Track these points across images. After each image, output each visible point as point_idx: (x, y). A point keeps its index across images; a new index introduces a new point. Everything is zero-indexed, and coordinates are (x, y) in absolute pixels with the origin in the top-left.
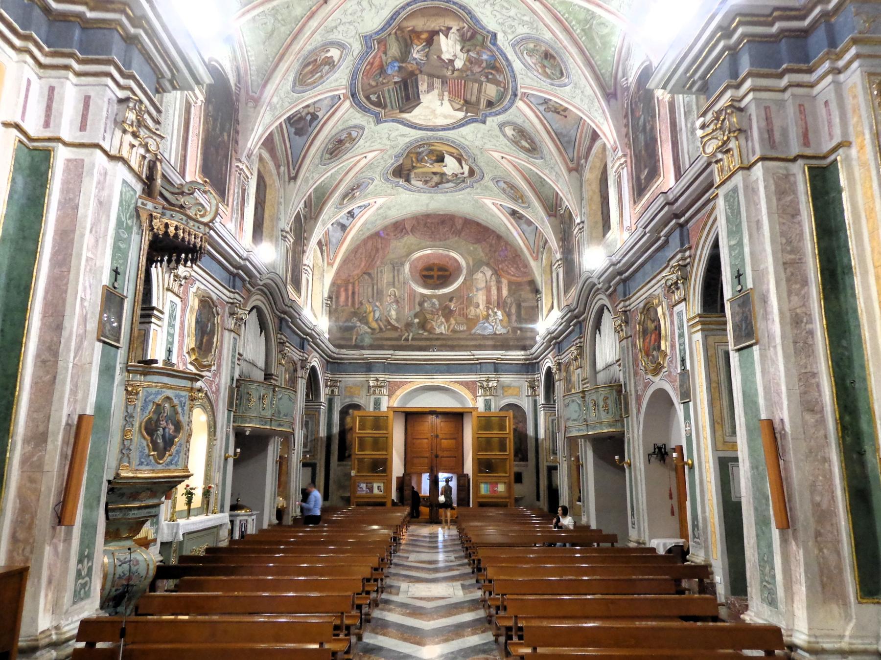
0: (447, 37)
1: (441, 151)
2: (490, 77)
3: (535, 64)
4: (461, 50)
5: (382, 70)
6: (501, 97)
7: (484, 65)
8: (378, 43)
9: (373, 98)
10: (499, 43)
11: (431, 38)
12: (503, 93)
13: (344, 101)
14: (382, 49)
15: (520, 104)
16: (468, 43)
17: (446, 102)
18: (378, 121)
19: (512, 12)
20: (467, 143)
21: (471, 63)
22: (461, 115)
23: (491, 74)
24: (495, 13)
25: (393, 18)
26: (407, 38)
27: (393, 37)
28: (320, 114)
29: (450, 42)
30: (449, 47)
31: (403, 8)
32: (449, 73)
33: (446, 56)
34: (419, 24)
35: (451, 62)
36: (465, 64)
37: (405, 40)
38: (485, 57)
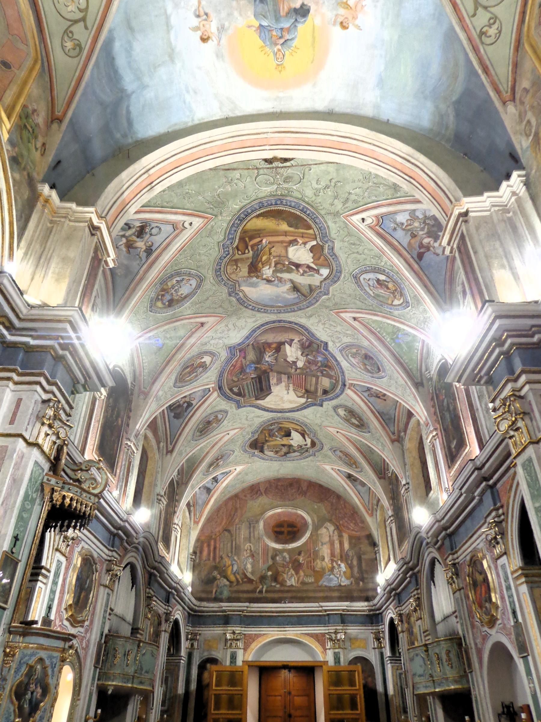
0: (291, 346)
1: (288, 428)
2: (324, 372)
4: (302, 355)
5: (242, 370)
6: (334, 387)
8: (240, 351)
9: (235, 390)
10: (329, 349)
11: (279, 347)
12: (335, 384)
13: (213, 392)
14: (243, 355)
15: (349, 392)
16: (307, 350)
18: (239, 407)
19: (339, 328)
20: (308, 421)
21: (309, 363)
22: (303, 400)
27: (251, 347)
28: (194, 403)
29: (293, 349)
30: (292, 352)
31: (259, 328)
32: (293, 371)
33: (290, 359)
34: (271, 338)
35: (295, 363)
36: (304, 364)
38: (320, 359)
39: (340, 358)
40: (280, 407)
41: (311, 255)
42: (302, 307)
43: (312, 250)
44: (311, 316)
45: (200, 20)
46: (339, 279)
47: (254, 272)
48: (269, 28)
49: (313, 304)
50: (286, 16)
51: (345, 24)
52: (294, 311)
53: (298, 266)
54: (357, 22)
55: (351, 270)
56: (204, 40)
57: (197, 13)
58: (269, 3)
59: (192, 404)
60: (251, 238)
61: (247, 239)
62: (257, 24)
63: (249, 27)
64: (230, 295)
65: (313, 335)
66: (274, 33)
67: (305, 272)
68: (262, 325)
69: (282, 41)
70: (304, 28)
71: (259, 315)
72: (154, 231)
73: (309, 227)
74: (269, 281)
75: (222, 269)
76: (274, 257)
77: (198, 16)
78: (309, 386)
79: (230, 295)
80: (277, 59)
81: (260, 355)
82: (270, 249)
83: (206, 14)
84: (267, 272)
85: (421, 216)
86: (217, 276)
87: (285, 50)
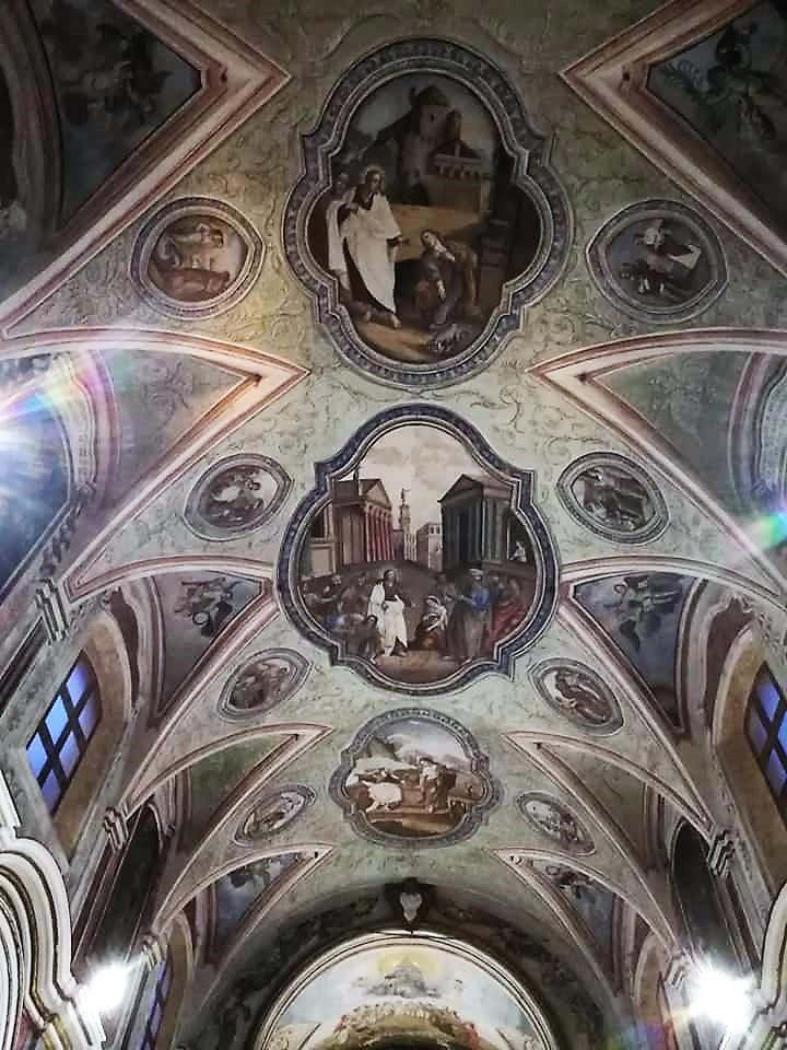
0: (397, 640)
1: (407, 323)
3: (270, 666)
4: (376, 619)
5: (496, 599)
6: (303, 564)
7: (340, 607)
9: (521, 553)
10: (325, 654)
11: (420, 636)
13: (572, 582)
14: (488, 641)
15: (270, 573)
16: (368, 635)
17: (396, 503)
18: (527, 478)
19: (318, 705)
20: (346, 376)
23: (326, 596)
24: (337, 692)
25: (466, 679)
26: (449, 641)
27: (472, 654)
30: (393, 623)
31: (451, 688)
33: (399, 605)
34: (434, 662)
35: (389, 597)
37: (455, 641)
38: (341, 620)
39: (305, 648)
40: (425, 431)
41: (371, 796)
42: (379, 720)
43: (372, 801)
44: (367, 706)
46: (332, 780)
47: (450, 776)
49: (362, 730)
52: (392, 712)
53: (388, 779)
55: (318, 802)
59: (625, 580)
60: (447, 815)
61: (451, 815)
64: (487, 758)
65: (358, 671)
67: (379, 774)
68: (445, 690)
71: (448, 711)
72: (555, 871)
73: (373, 824)
74: (429, 760)
75: (488, 800)
76: (419, 790)
78: (356, 527)
79: (487, 758)
81: (455, 629)
82: (424, 799)
84: (430, 772)
85: (256, 877)
86: (498, 792)
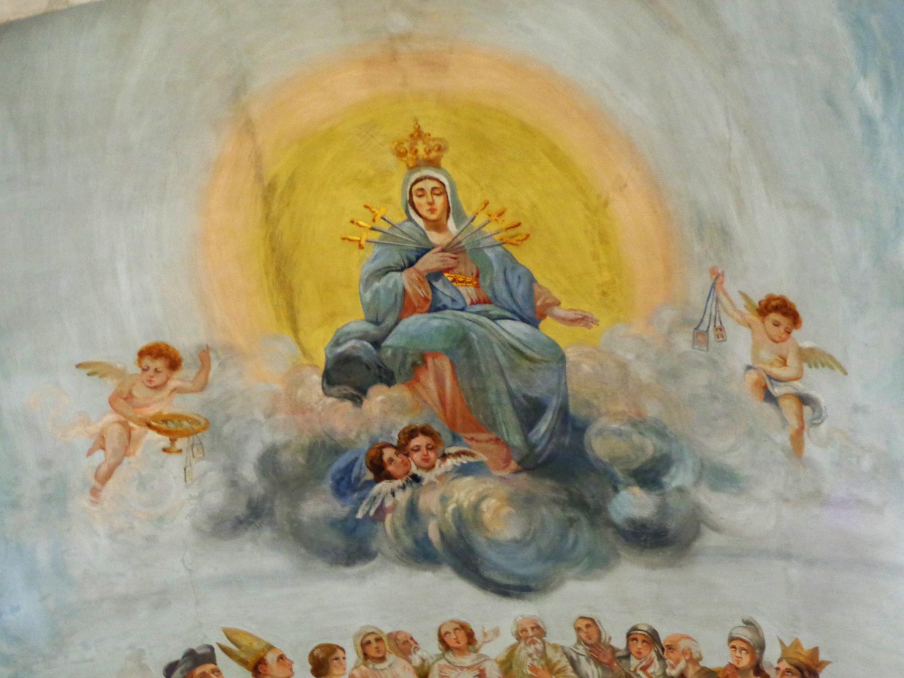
45: (799, 386)
48: (496, 311)
50: (423, 357)
51: (159, 364)
54: (109, 386)
56: (780, 310)
57: (807, 410)
58: (505, 399)
62: (549, 328)
63: (583, 320)
66: (468, 292)
69: (430, 262)
70: (339, 314)
77: (803, 400)
80: (440, 190)
83: (769, 397)
87: (407, 227)
